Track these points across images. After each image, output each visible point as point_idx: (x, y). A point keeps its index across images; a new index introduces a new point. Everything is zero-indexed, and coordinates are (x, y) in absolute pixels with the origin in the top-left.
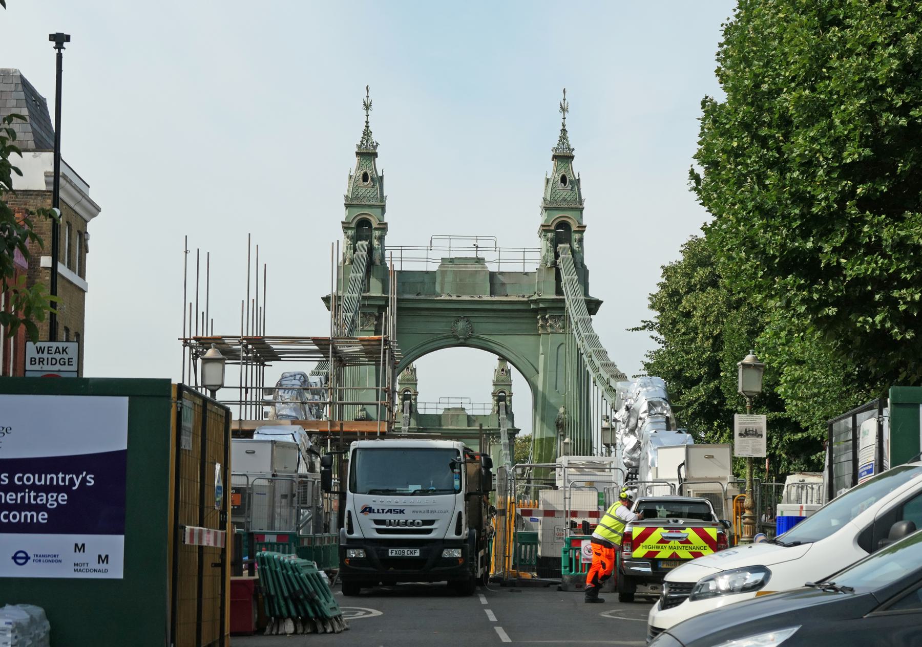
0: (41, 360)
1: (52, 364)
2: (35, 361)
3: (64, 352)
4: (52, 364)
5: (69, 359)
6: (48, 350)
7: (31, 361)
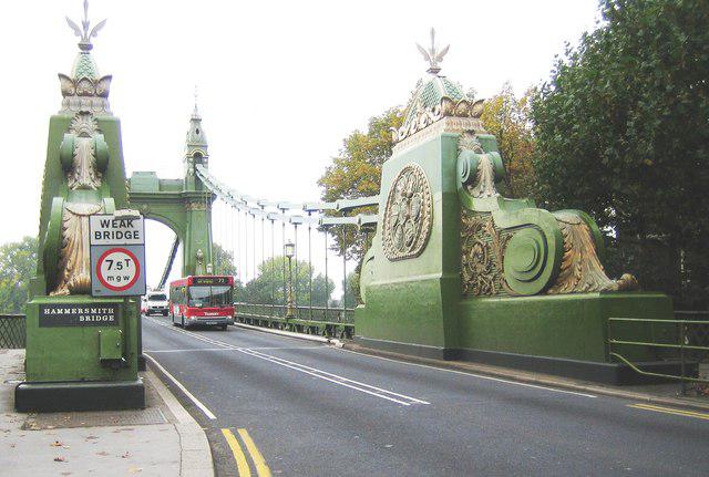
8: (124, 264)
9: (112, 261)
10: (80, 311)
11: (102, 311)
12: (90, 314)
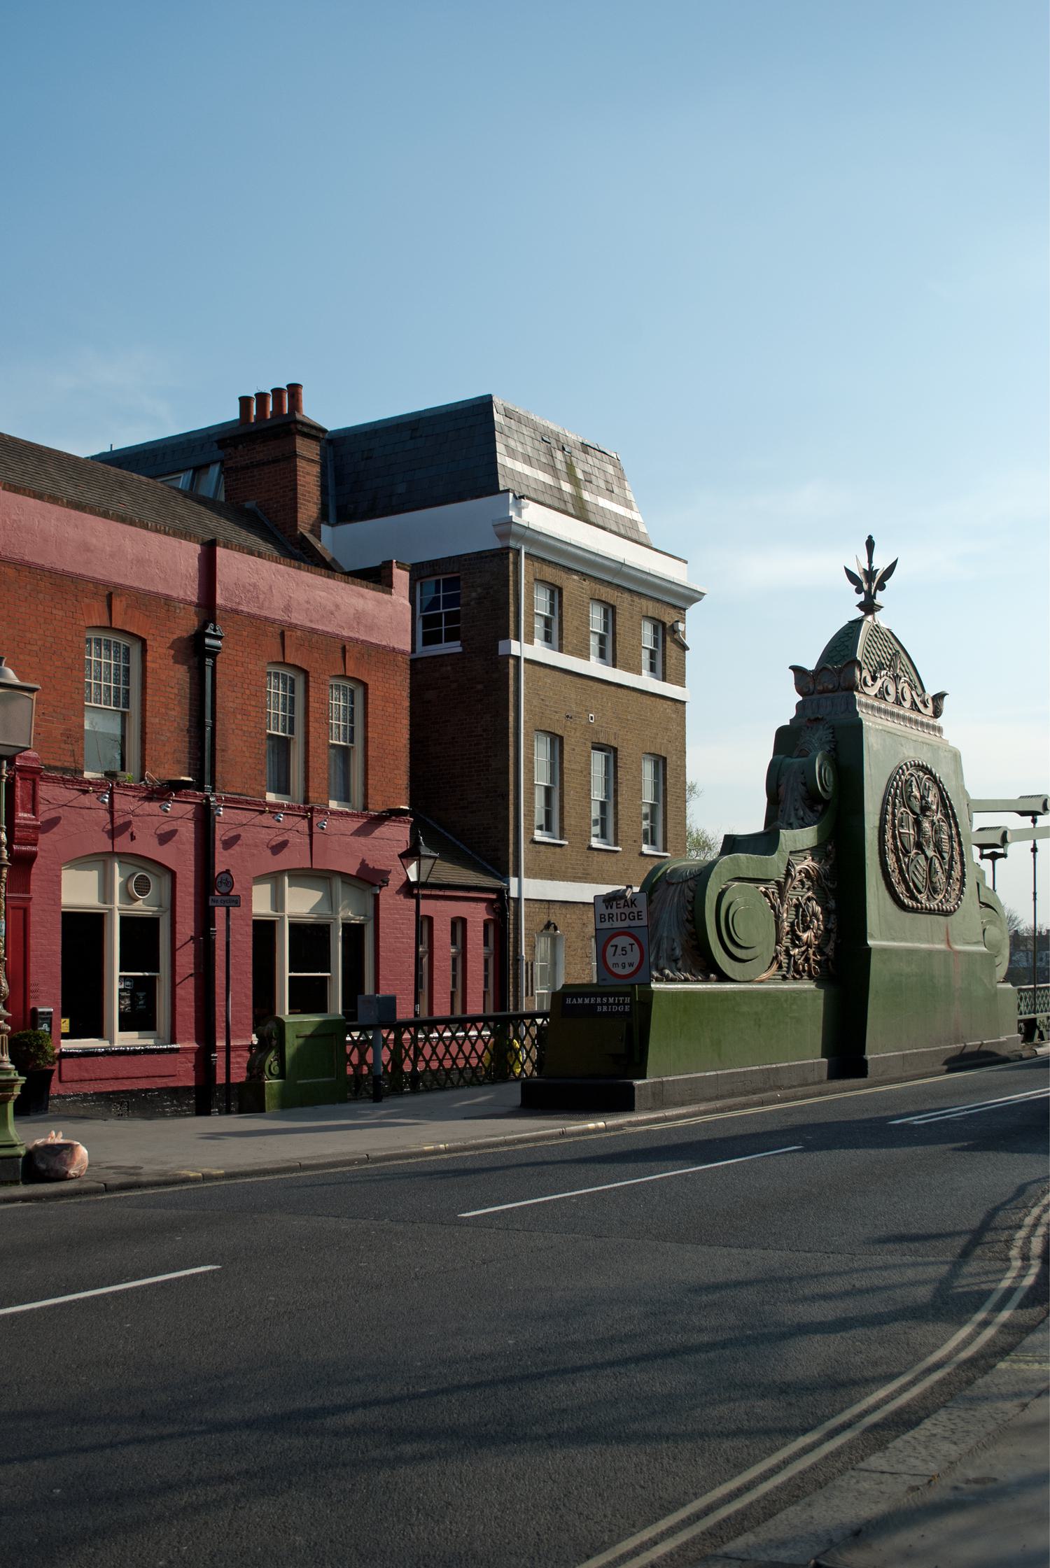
2: (604, 918)
5: (638, 912)
8: (629, 948)
9: (616, 946)
10: (599, 1000)
11: (619, 1001)
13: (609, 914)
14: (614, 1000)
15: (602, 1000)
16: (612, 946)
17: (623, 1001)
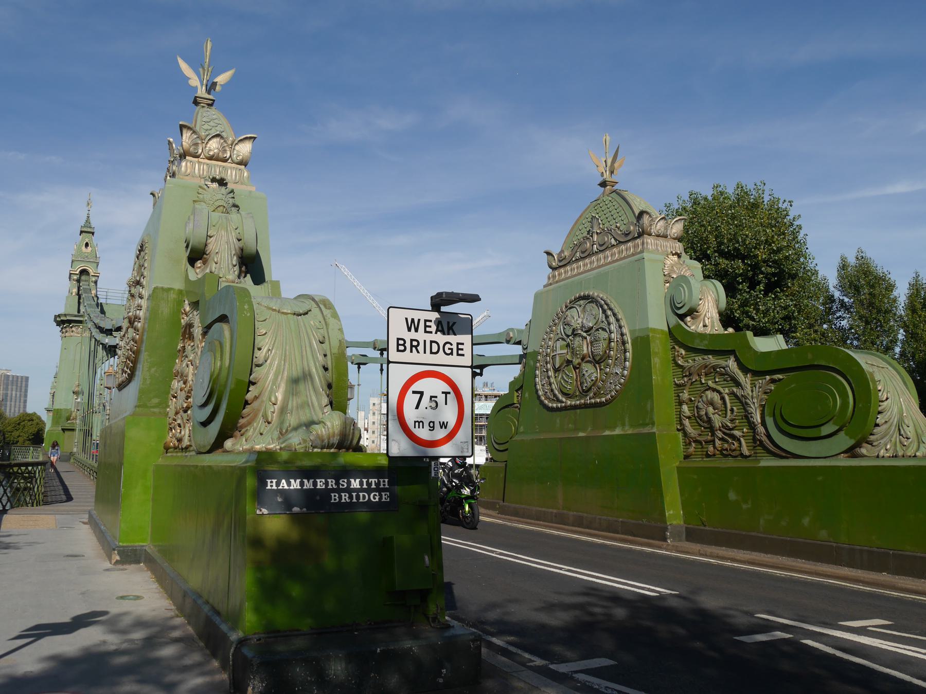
0: (415, 343)
1: (431, 353)
2: (404, 345)
3: (451, 331)
4: (431, 353)
5: (458, 344)
6: (426, 326)
7: (398, 345)
8: (441, 399)
9: (421, 393)
10: (332, 483)
11: (369, 484)
12: (349, 490)
13: (412, 340)
14: (361, 483)
15: (337, 483)
16: (414, 392)
17: (378, 484)
